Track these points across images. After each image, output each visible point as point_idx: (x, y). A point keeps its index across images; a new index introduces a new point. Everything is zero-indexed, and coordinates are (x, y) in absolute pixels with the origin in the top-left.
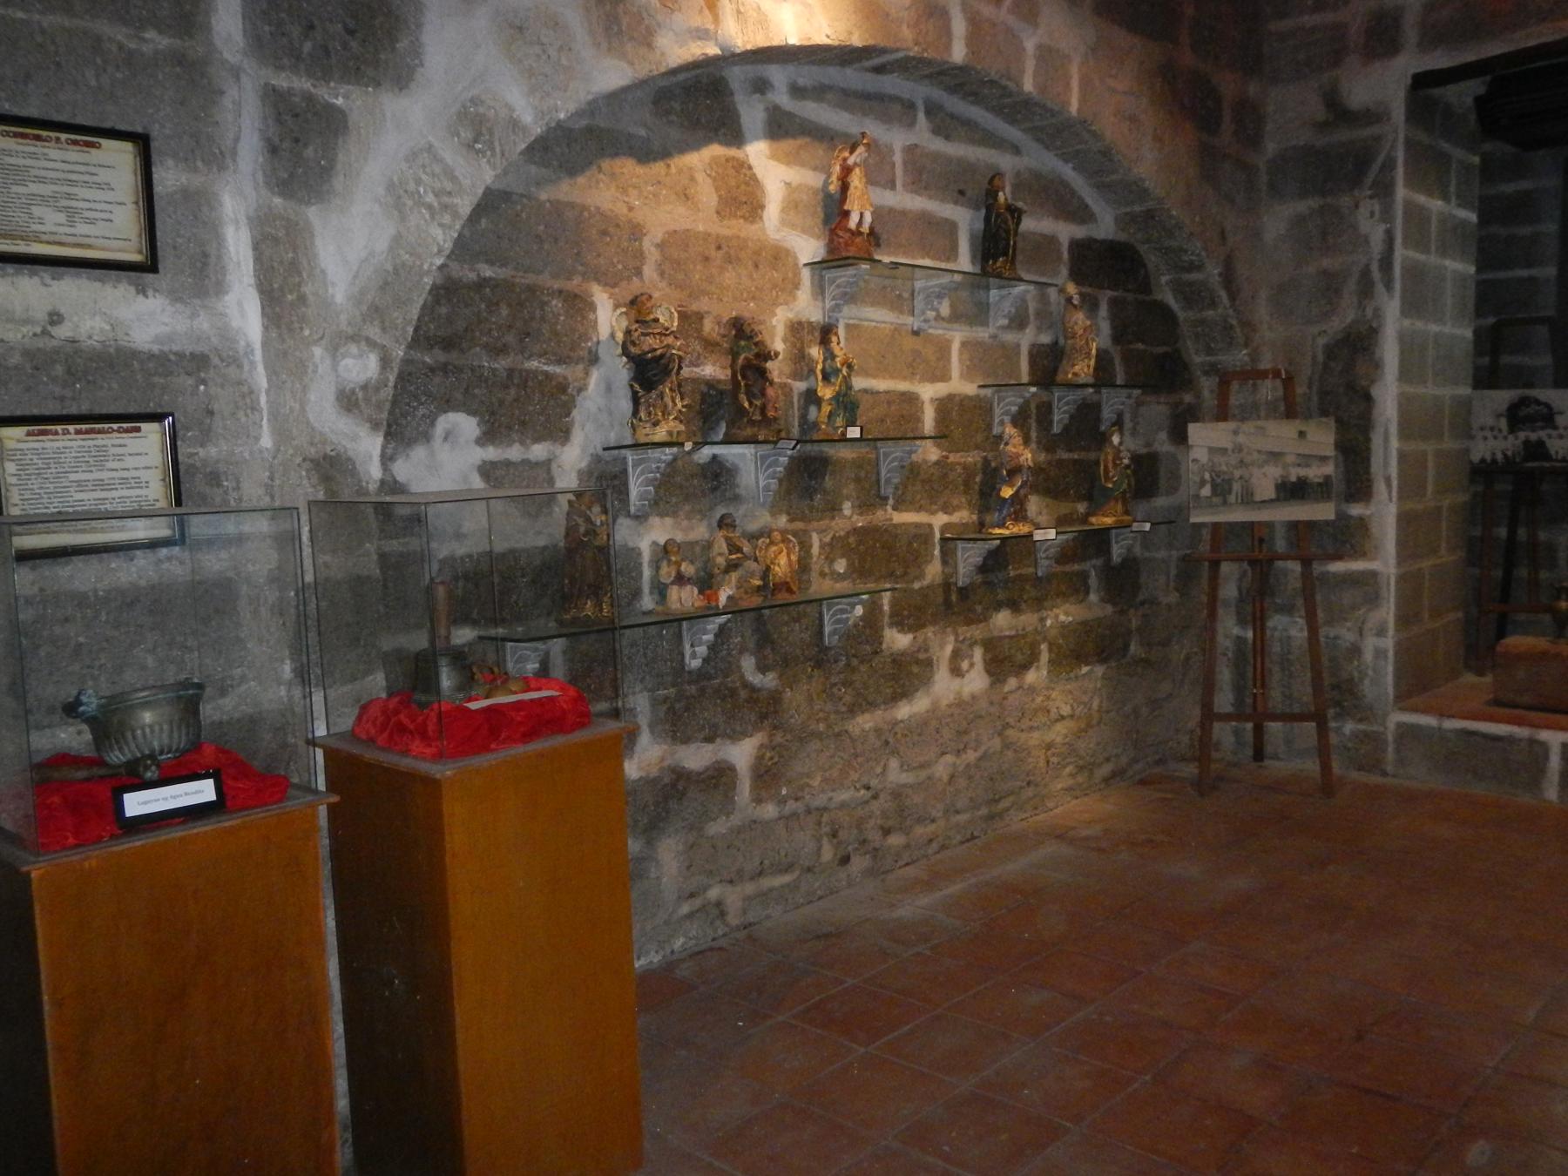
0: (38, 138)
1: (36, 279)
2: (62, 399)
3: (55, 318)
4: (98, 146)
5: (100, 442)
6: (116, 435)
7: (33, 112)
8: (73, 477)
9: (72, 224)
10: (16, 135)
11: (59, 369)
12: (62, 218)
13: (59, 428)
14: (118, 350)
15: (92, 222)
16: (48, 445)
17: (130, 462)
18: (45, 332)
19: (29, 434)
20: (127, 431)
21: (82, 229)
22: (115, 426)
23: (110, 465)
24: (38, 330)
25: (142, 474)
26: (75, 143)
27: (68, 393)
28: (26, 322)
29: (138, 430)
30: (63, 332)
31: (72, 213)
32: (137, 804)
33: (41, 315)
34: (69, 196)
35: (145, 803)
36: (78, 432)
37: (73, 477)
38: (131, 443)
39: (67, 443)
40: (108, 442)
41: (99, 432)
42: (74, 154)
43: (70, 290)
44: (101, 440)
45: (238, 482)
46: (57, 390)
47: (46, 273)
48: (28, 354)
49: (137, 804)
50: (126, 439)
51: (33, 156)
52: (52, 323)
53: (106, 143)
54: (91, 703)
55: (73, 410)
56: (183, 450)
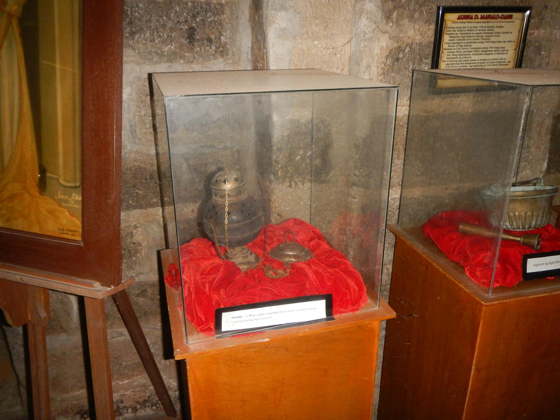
5: (490, 25)
6: (500, 20)
8: (474, 45)
13: (473, 14)
16: (466, 25)
17: (503, 37)
19: (459, 18)
20: (506, 18)
22: (500, 14)
23: (492, 39)
29: (511, 17)
35: (537, 265)
36: (482, 18)
37: (474, 45)
40: (495, 24)
41: (493, 18)
44: (492, 23)
45: (550, 53)
49: (534, 265)
56: (530, 31)
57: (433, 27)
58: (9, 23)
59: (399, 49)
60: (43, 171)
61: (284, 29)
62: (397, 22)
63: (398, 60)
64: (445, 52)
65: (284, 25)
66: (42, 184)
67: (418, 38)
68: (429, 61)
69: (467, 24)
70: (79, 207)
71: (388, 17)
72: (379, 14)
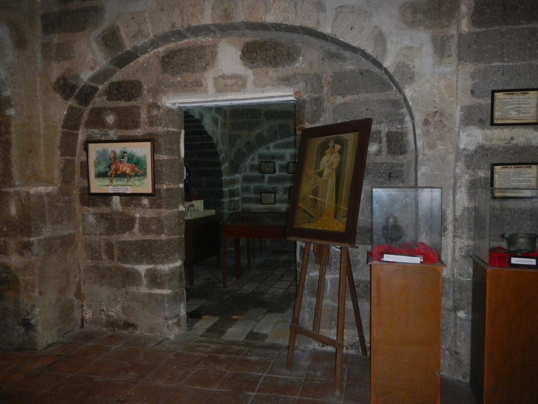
0: (512, 94)
1: (508, 129)
2: (511, 159)
3: (512, 138)
4: (528, 93)
7: (512, 88)
8: (512, 179)
9: (519, 114)
10: (507, 94)
11: (512, 152)
12: (516, 113)
14: (528, 146)
15: (524, 113)
17: (527, 176)
18: (509, 142)
21: (522, 115)
23: (522, 176)
24: (507, 142)
25: (531, 179)
26: (522, 93)
27: (513, 157)
28: (505, 140)
29: (531, 167)
30: (514, 142)
31: (519, 112)
32: (514, 261)
33: (508, 137)
34: (519, 107)
36: (514, 167)
37: (512, 179)
38: (529, 170)
39: (512, 170)
42: (521, 97)
43: (516, 132)
44: (520, 170)
46: (510, 157)
47: (511, 127)
48: (504, 148)
49: (514, 261)
50: (527, 169)
51: (511, 98)
52: (511, 140)
53: (530, 92)
54: (507, 235)
55: (514, 162)
57: (490, 171)
58: (333, 171)
59: (474, 180)
60: (336, 212)
61: (424, 173)
62: (473, 170)
63: (474, 184)
64: (497, 182)
65: (424, 171)
66: (335, 216)
67: (483, 175)
68: (489, 185)
69: (507, 170)
70: (345, 222)
71: (468, 168)
72: (464, 167)
